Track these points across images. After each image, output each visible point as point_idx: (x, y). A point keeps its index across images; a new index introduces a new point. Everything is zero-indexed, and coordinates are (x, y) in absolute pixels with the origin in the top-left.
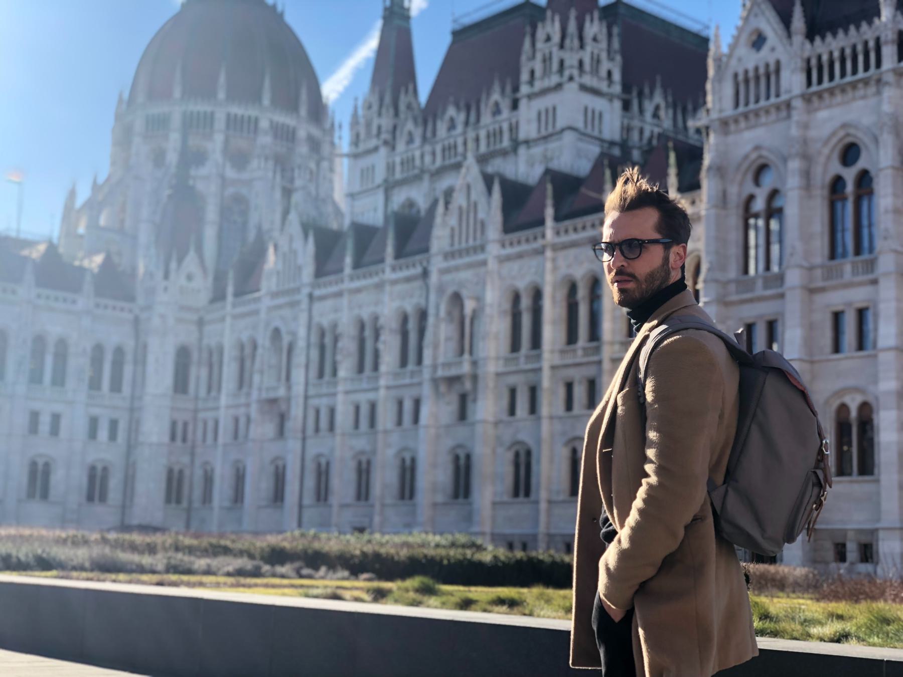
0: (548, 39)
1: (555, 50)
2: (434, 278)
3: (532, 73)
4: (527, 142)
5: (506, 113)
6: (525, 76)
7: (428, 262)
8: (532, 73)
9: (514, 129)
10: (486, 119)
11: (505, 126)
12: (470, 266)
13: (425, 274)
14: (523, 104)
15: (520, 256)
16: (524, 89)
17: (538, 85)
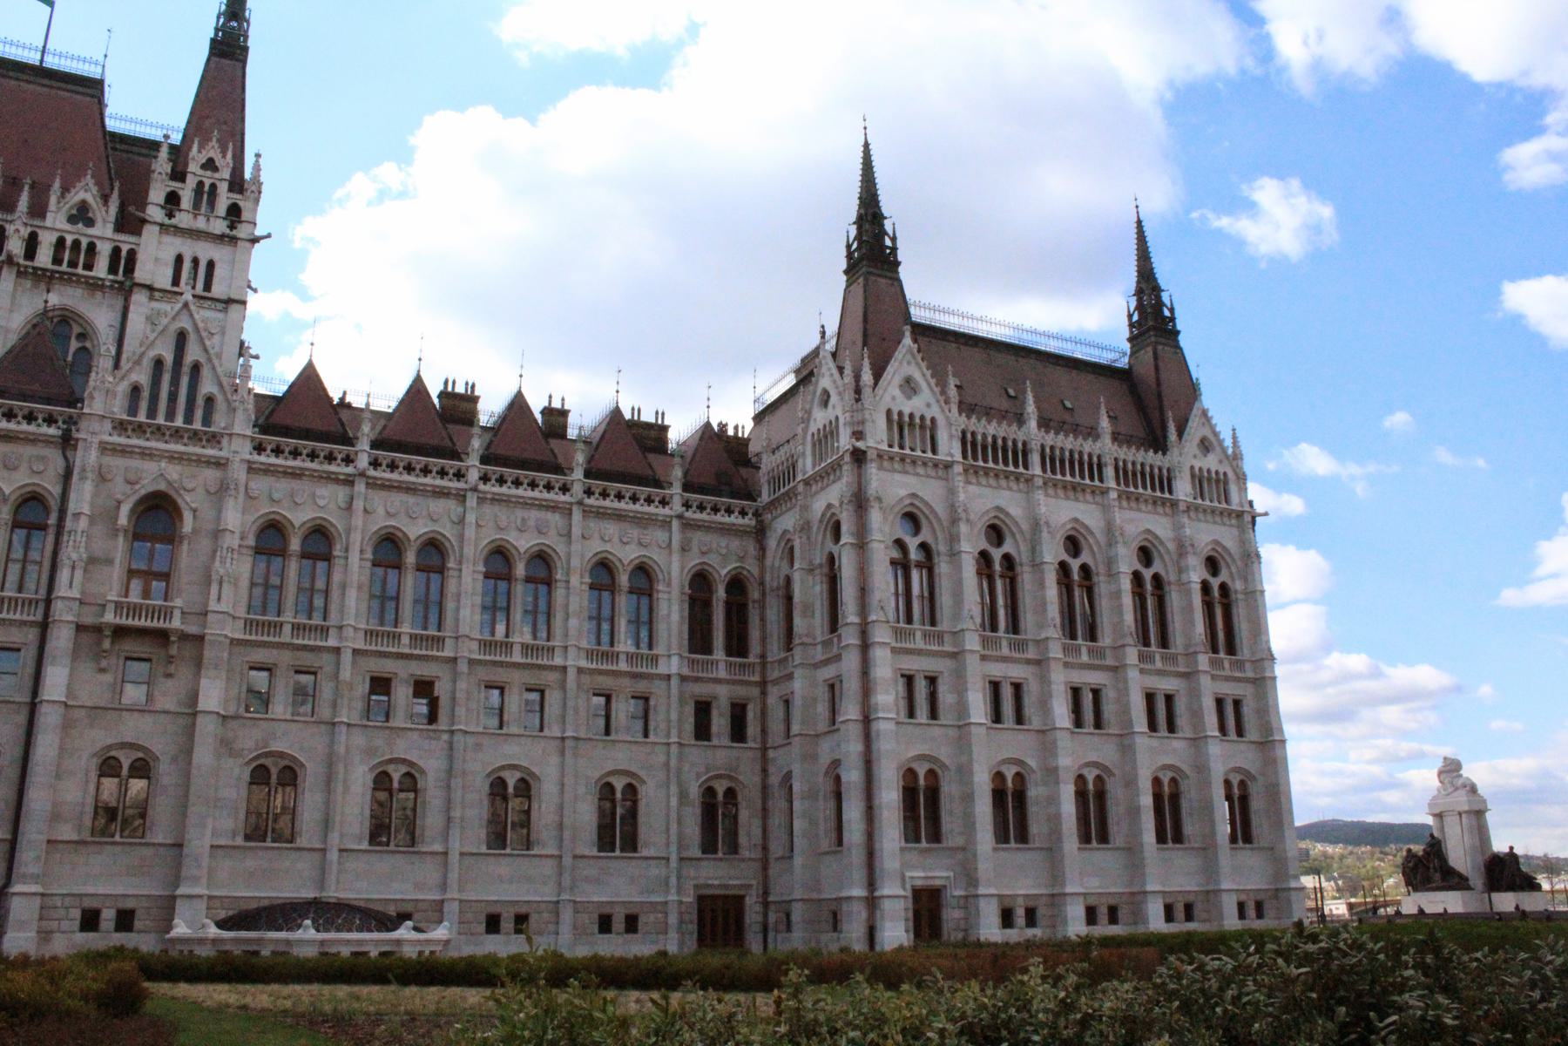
0: (210, 165)
1: (223, 188)
2: (87, 457)
3: (173, 199)
4: (150, 288)
5: (103, 230)
6: (157, 194)
7: (71, 421)
8: (173, 199)
9: (123, 263)
10: (56, 220)
11: (104, 249)
12: (173, 458)
13: (67, 442)
14: (150, 233)
15: (296, 474)
16: (155, 213)
17: (183, 219)
